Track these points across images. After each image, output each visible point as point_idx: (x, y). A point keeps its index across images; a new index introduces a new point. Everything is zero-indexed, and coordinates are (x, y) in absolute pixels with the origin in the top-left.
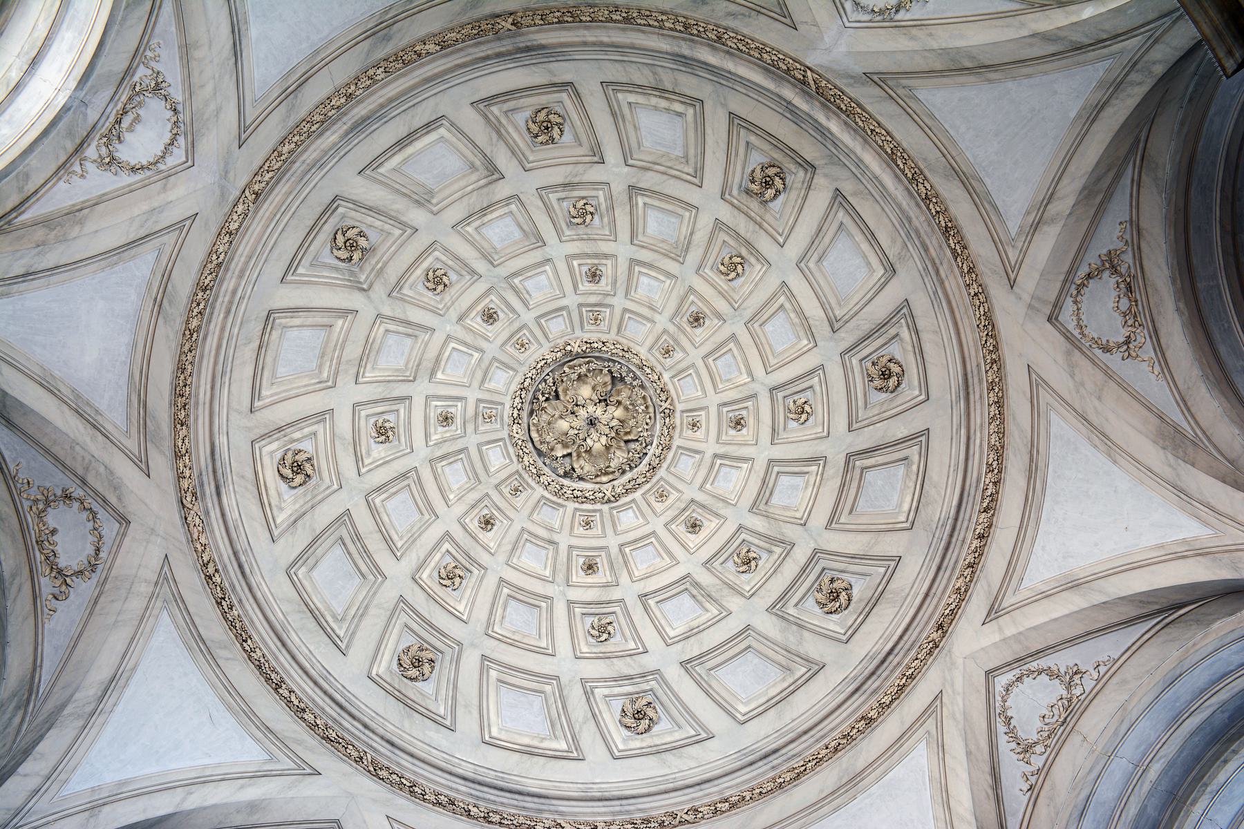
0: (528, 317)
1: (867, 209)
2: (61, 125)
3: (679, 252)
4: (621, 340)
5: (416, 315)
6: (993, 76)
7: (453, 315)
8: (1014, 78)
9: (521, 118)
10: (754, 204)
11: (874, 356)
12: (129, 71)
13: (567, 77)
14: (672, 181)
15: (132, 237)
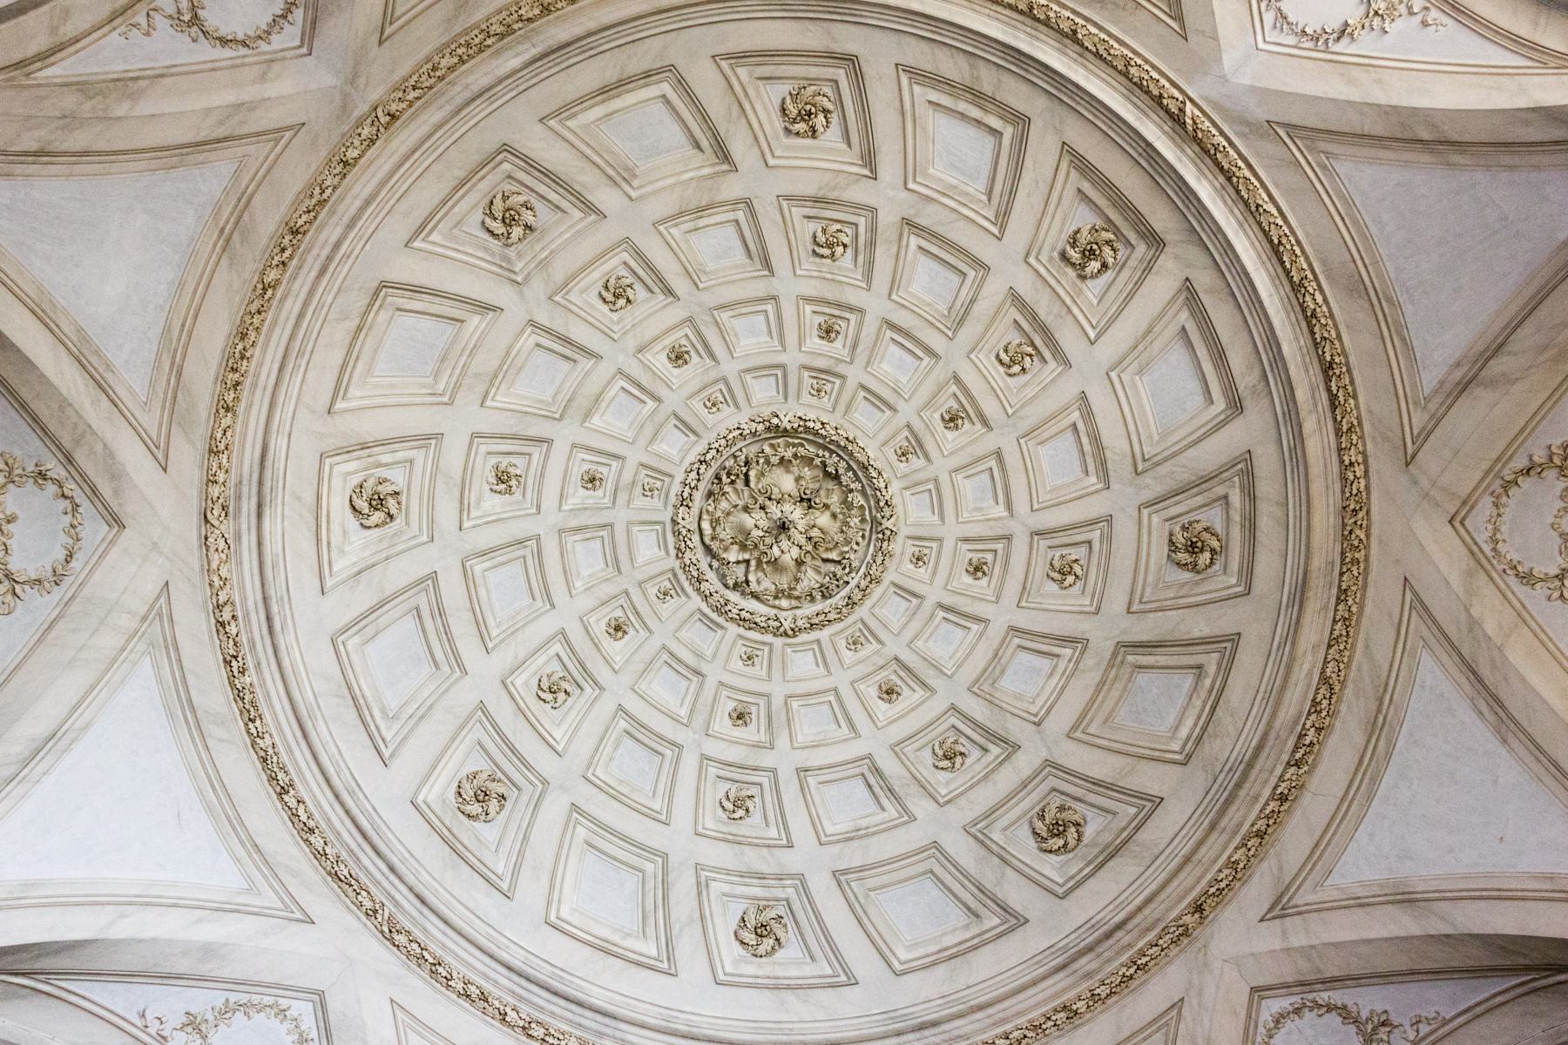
4: (846, 425)
5: (579, 333)
6: (1456, 158)
7: (631, 343)
8: (1488, 167)
11: (1186, 519)
13: (851, 48)
14: (962, 224)
15: (204, 135)
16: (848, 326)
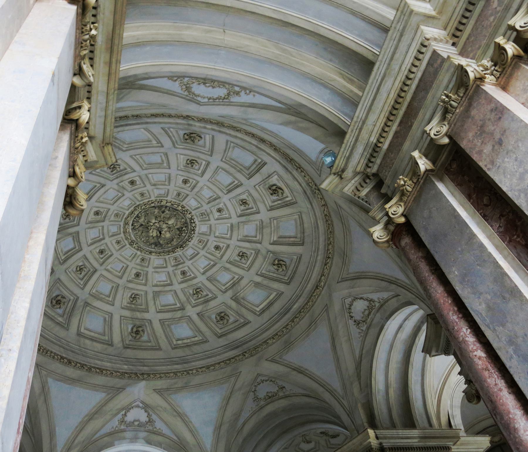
0: (202, 253)
1: (98, 347)
2: (388, 313)
3: (156, 294)
4: (163, 257)
5: (247, 245)
6: (86, 418)
7: (232, 247)
8: (80, 422)
9: (232, 319)
10: (138, 323)
11: (66, 304)
12: (368, 328)
14: (170, 317)
15: (358, 280)
16: (180, 277)
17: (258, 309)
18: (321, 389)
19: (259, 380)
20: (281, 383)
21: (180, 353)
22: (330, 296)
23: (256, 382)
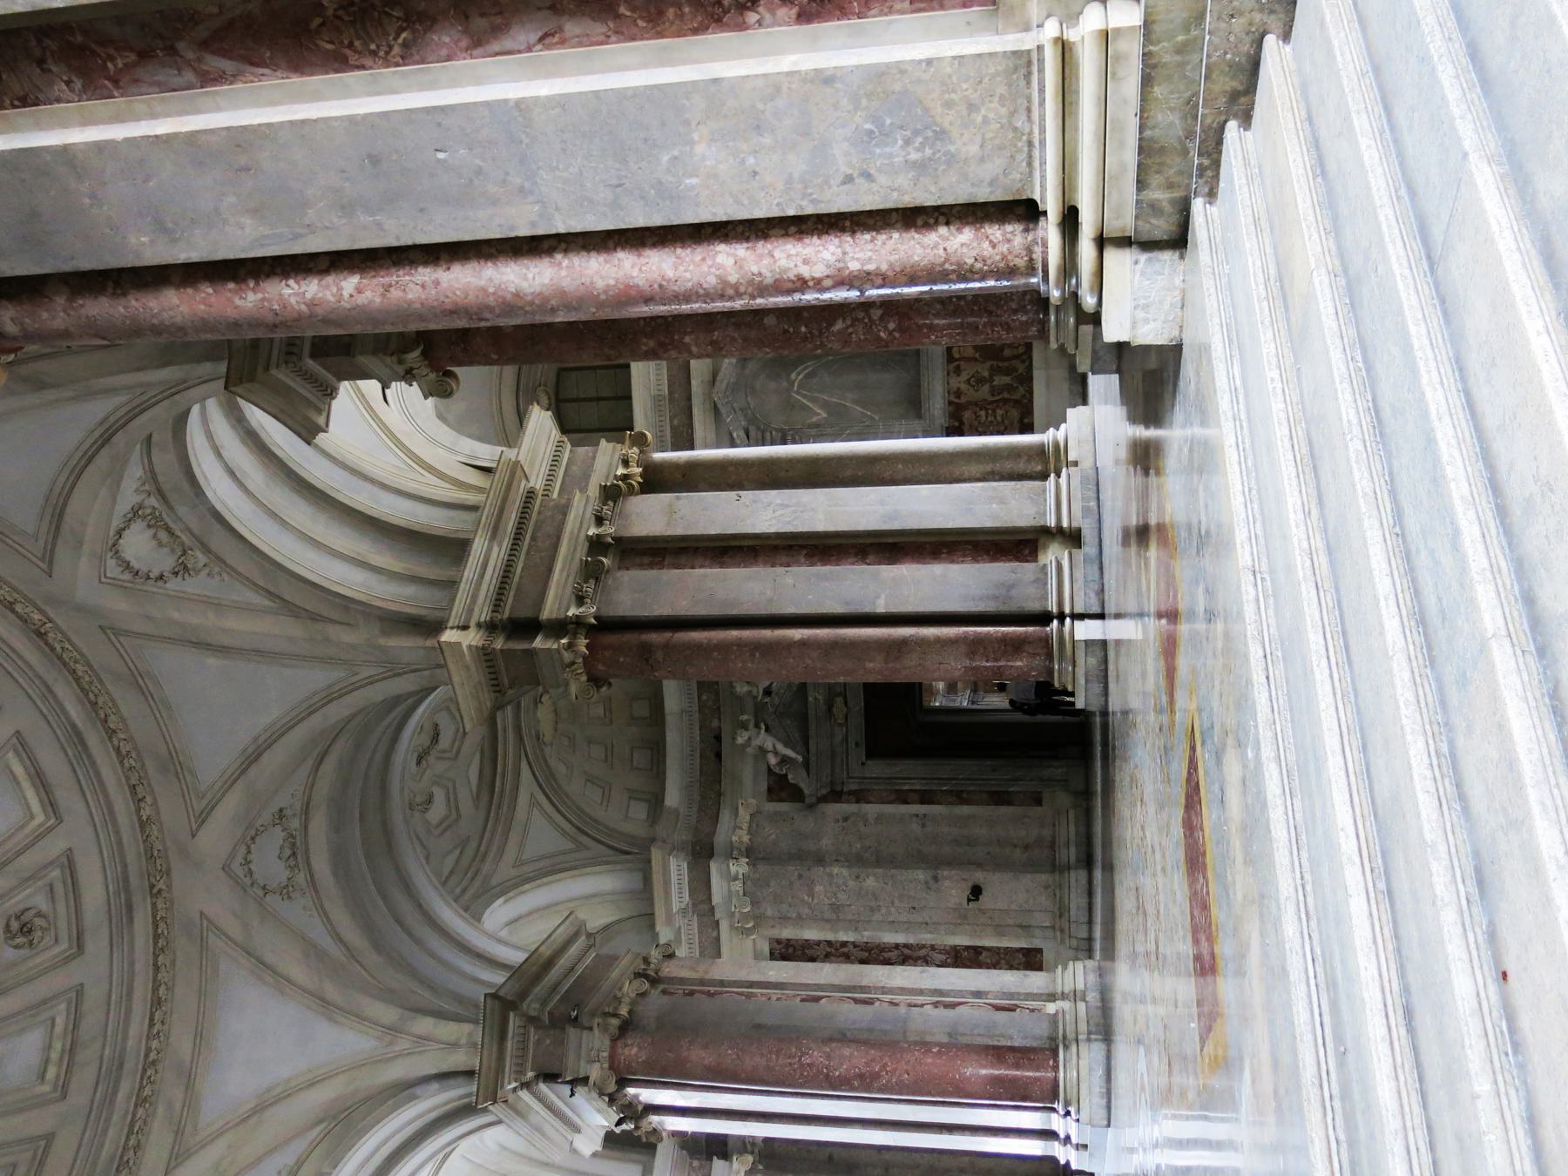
2: (186, 486)
9: (41, 902)
12: (206, 549)
13: (90, 946)
15: (67, 518)
17: (40, 818)
18: (316, 721)
19: (240, 872)
20: (266, 817)
21: (84, 1078)
22: (81, 609)
23: (245, 882)
